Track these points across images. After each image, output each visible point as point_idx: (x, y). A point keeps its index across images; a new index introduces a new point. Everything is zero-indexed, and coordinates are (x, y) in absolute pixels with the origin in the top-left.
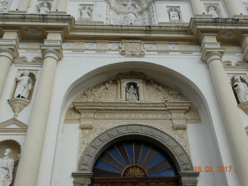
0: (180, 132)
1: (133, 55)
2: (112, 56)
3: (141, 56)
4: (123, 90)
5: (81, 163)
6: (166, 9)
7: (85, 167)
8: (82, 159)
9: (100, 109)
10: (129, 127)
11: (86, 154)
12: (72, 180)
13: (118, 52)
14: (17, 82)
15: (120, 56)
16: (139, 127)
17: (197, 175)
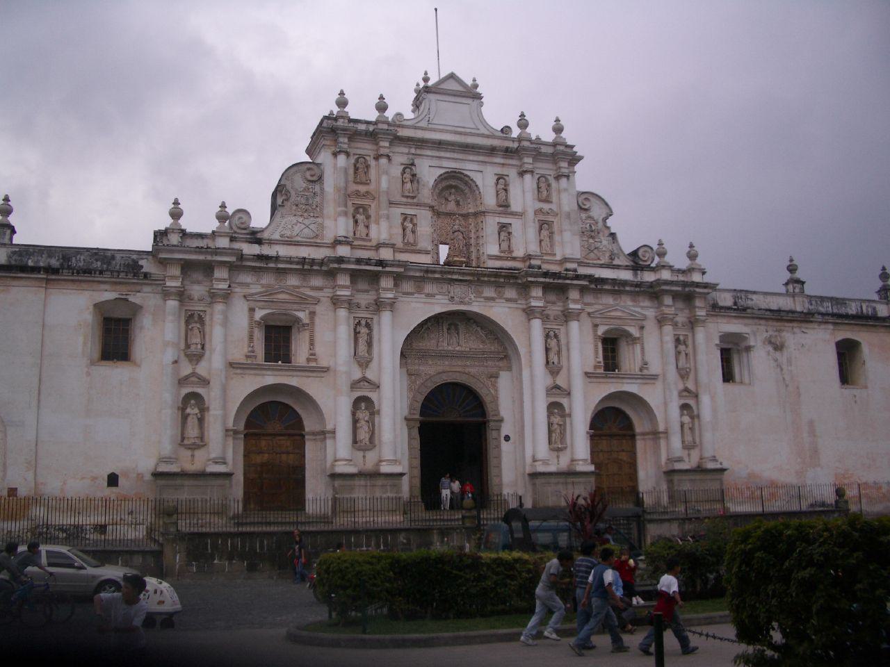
0: (493, 380)
1: (462, 303)
2: (440, 305)
3: (469, 304)
4: (445, 330)
5: (411, 408)
6: (496, 228)
7: (415, 412)
8: (411, 405)
9: (424, 355)
10: (450, 374)
11: (414, 399)
12: (405, 423)
13: (446, 297)
14: (356, 333)
15: (447, 301)
16: (458, 374)
17: (501, 420)
